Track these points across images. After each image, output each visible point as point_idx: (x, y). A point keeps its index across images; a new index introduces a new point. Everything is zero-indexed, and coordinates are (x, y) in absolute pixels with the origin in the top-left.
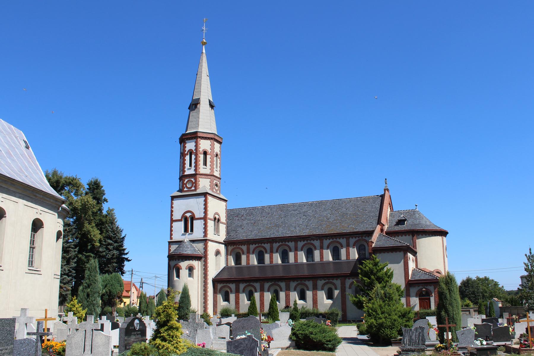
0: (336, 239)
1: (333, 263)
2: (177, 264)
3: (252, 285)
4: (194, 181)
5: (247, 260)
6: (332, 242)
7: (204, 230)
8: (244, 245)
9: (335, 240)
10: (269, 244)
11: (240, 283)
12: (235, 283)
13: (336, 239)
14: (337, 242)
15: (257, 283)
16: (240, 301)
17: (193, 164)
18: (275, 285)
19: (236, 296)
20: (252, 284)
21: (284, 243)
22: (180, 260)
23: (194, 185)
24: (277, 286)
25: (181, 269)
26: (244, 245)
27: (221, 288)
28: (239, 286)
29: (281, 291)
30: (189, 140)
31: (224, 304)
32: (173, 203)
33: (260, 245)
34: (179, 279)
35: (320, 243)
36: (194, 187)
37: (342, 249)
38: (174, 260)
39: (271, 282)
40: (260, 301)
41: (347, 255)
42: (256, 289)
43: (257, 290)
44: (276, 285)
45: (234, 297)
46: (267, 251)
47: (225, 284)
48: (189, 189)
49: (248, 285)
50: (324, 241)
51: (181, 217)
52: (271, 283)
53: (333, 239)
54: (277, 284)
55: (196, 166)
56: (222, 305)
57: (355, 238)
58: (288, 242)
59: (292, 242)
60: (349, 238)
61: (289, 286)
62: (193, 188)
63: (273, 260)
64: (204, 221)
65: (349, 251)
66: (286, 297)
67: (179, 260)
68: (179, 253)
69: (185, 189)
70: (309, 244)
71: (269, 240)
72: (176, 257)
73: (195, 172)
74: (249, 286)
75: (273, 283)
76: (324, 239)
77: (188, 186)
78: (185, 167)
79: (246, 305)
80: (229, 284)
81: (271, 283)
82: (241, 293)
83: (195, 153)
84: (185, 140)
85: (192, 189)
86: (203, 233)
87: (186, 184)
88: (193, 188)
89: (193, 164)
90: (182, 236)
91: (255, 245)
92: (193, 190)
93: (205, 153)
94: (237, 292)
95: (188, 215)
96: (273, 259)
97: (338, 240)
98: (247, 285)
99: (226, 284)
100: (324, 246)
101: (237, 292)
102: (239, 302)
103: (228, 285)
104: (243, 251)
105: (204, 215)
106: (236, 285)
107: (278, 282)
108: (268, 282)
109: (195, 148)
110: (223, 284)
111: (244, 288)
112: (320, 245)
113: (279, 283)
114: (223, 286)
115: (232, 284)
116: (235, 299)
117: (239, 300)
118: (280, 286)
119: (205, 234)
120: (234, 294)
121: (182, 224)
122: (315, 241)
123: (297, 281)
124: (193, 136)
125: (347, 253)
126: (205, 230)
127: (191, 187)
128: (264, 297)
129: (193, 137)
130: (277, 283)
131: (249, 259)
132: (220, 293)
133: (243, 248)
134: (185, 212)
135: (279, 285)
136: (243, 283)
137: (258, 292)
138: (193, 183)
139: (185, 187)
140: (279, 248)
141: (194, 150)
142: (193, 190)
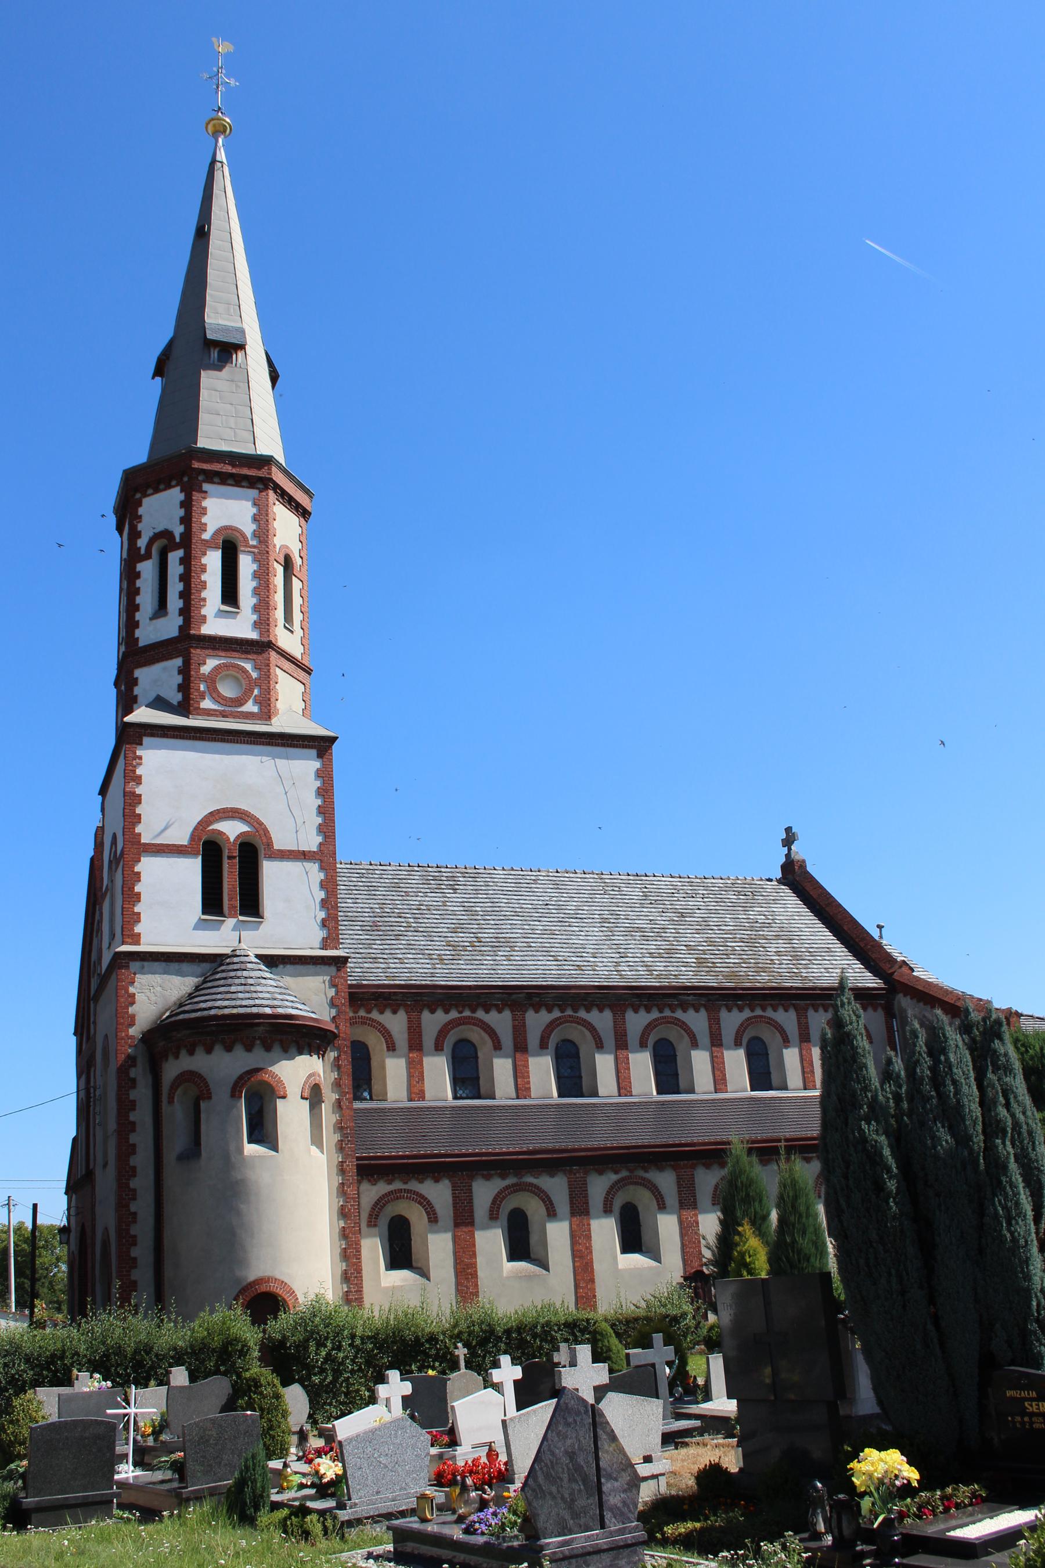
0: (764, 1009)
1: (558, 1106)
2: (262, 1069)
3: (531, 1185)
4: (254, 675)
5: (410, 1076)
6: (749, 1019)
7: (322, 915)
8: (395, 1012)
9: (758, 1012)
10: (507, 1014)
11: (472, 1178)
12: (450, 1178)
13: (764, 1009)
14: (768, 1023)
15: (552, 1176)
16: (478, 1260)
17: (174, 603)
18: (636, 1183)
19: (455, 1240)
20: (530, 1179)
21: (569, 1012)
22: (293, 1050)
23: (256, 692)
24: (645, 1186)
25: (284, 1097)
26: (395, 1012)
27: (377, 1203)
28: (470, 1191)
29: (662, 1207)
30: (165, 489)
31: (398, 1283)
32: (140, 758)
33: (467, 1013)
34: (275, 1148)
35: (709, 1019)
36: (256, 702)
37: (787, 1047)
38: (183, 1053)
39: (616, 1172)
40: (574, 1256)
41: (803, 1072)
42: (552, 1204)
43: (558, 1211)
44: (641, 1184)
45: (450, 1246)
46: (499, 1042)
47: (397, 1185)
48: (231, 707)
49: (513, 1185)
50: (724, 1014)
51: (261, 824)
52: (614, 1177)
53: (752, 1010)
54: (644, 1179)
55: (186, 612)
56: (387, 1288)
57: (741, 1009)
58: (588, 1011)
59: (601, 1010)
60: (806, 1010)
61: (693, 1184)
62: (250, 707)
63: (529, 1083)
64: (322, 868)
65: (811, 1055)
66: (682, 1235)
67: (268, 1048)
68: (268, 1011)
69: (207, 704)
70: (669, 1023)
71: (514, 997)
72: (261, 1028)
73: (261, 634)
74: (515, 1191)
75: (624, 1173)
76: (721, 1005)
77: (227, 690)
78: (204, 600)
79: (508, 1278)
80: (421, 1182)
81: (614, 1177)
82: (598, 1217)
83: (254, 547)
84: (201, 478)
85: (245, 708)
86: (318, 928)
87: (211, 680)
88: (250, 707)
89: (174, 603)
90: (194, 929)
91: (447, 1012)
92: (249, 716)
93: (288, 563)
94: (580, 1209)
95: (232, 830)
96: (529, 1077)
97: (770, 1013)
98: (507, 1187)
99: (406, 1183)
100: (723, 1032)
101: (580, 1209)
102: (474, 1265)
103: (414, 1185)
104: (390, 1036)
105: (320, 839)
106: (454, 1188)
107: (646, 1171)
108: (601, 1173)
109: (254, 527)
110: (390, 1182)
111: (494, 1202)
112: (710, 1027)
113: (647, 1175)
114: (391, 1193)
115: (437, 1181)
116: (455, 1253)
117: (474, 1255)
118: (656, 1188)
119: (329, 934)
120: (445, 1231)
121: (192, 869)
122: (691, 1012)
123: (503, 1177)
124: (245, 471)
125: (717, 1073)
126: (328, 915)
127: (240, 702)
128: (589, 1237)
129: (246, 478)
130: (641, 1173)
131: (422, 1074)
132: (375, 1226)
133: (388, 1026)
134: (211, 813)
135: (649, 1181)
136: (488, 1178)
137: (561, 1220)
138: (252, 684)
139: (204, 692)
140: (552, 1031)
141: (249, 535)
142: (249, 716)
